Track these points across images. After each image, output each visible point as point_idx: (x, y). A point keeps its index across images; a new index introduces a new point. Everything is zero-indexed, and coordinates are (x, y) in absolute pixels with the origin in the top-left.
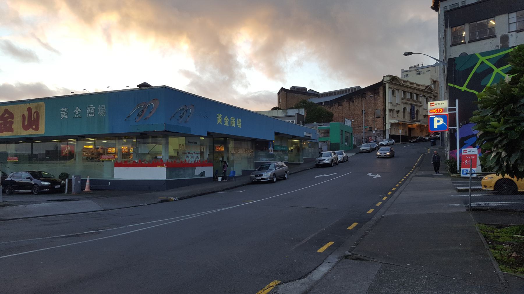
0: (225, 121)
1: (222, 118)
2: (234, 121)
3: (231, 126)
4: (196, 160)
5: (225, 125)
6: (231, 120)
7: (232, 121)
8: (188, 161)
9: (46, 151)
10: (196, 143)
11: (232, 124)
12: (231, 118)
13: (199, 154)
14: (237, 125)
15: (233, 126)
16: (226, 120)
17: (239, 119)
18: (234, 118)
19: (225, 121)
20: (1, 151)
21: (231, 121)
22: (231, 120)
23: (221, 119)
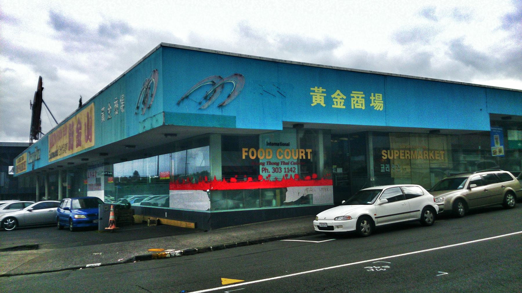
0: (334, 100)
1: (325, 95)
2: (362, 98)
3: (353, 108)
4: (287, 175)
5: (333, 106)
6: (353, 97)
7: (356, 99)
8: (267, 178)
9: (315, 88)
10: (288, 145)
11: (356, 105)
12: (353, 92)
13: (294, 164)
14: (371, 105)
15: (360, 107)
16: (339, 97)
17: (343, 101)
18: (362, 93)
19: (334, 100)
20: (1, 143)
21: (352, 99)
22: (353, 97)
23: (323, 98)
